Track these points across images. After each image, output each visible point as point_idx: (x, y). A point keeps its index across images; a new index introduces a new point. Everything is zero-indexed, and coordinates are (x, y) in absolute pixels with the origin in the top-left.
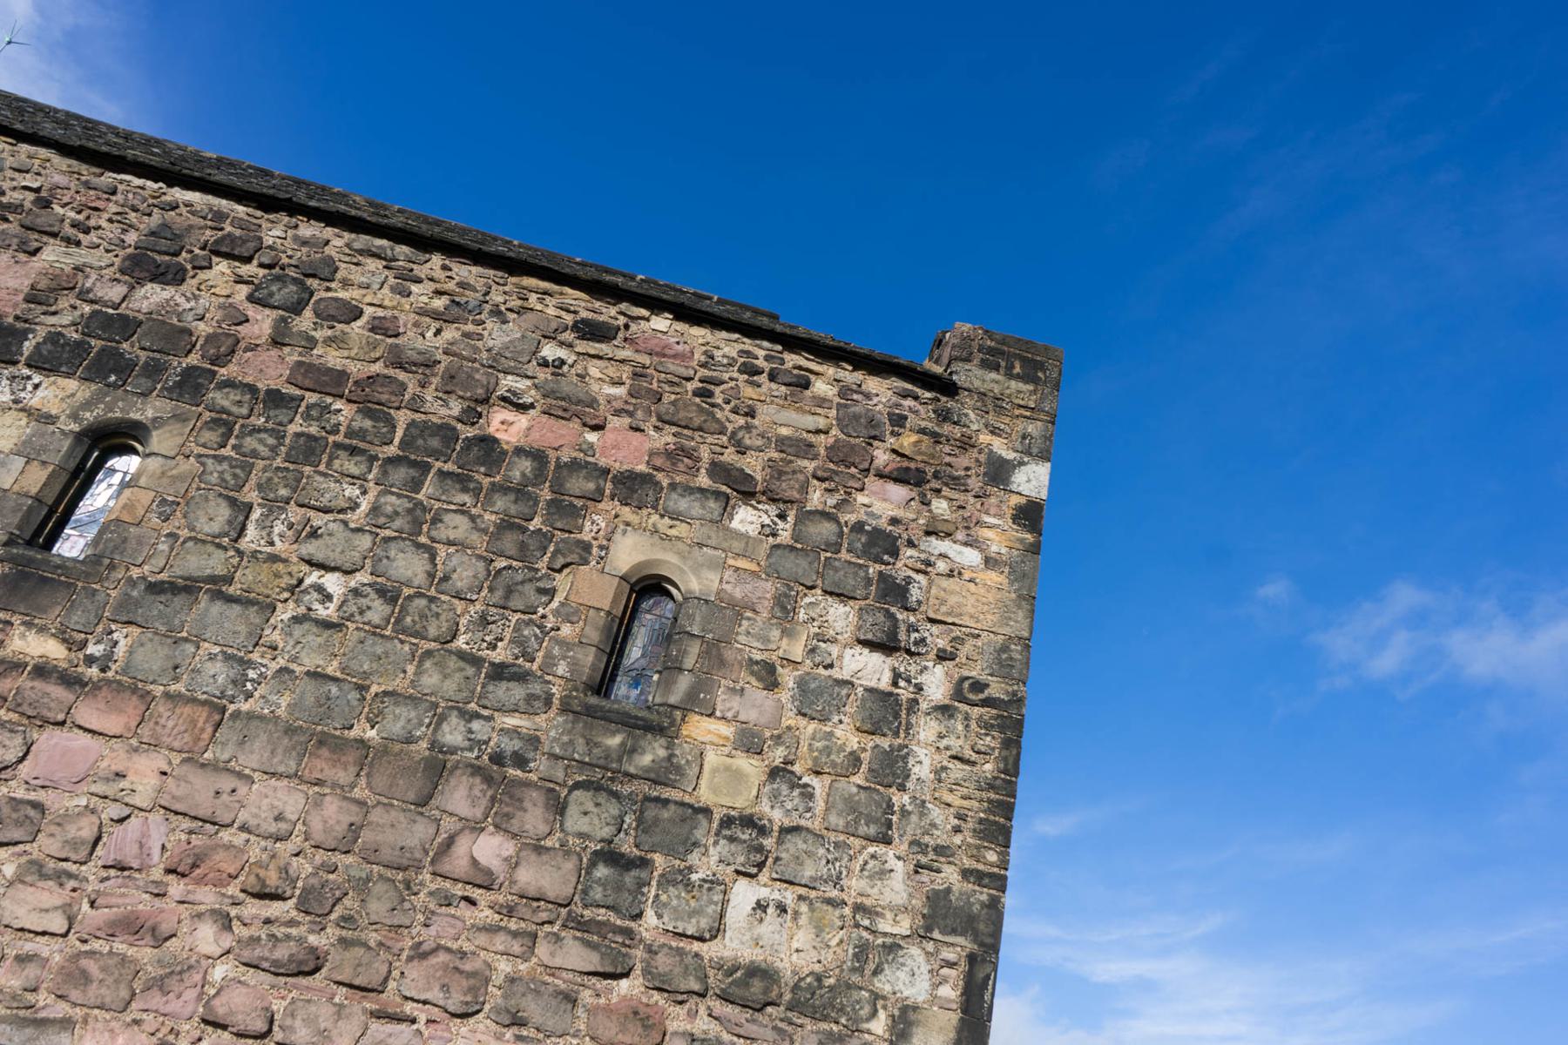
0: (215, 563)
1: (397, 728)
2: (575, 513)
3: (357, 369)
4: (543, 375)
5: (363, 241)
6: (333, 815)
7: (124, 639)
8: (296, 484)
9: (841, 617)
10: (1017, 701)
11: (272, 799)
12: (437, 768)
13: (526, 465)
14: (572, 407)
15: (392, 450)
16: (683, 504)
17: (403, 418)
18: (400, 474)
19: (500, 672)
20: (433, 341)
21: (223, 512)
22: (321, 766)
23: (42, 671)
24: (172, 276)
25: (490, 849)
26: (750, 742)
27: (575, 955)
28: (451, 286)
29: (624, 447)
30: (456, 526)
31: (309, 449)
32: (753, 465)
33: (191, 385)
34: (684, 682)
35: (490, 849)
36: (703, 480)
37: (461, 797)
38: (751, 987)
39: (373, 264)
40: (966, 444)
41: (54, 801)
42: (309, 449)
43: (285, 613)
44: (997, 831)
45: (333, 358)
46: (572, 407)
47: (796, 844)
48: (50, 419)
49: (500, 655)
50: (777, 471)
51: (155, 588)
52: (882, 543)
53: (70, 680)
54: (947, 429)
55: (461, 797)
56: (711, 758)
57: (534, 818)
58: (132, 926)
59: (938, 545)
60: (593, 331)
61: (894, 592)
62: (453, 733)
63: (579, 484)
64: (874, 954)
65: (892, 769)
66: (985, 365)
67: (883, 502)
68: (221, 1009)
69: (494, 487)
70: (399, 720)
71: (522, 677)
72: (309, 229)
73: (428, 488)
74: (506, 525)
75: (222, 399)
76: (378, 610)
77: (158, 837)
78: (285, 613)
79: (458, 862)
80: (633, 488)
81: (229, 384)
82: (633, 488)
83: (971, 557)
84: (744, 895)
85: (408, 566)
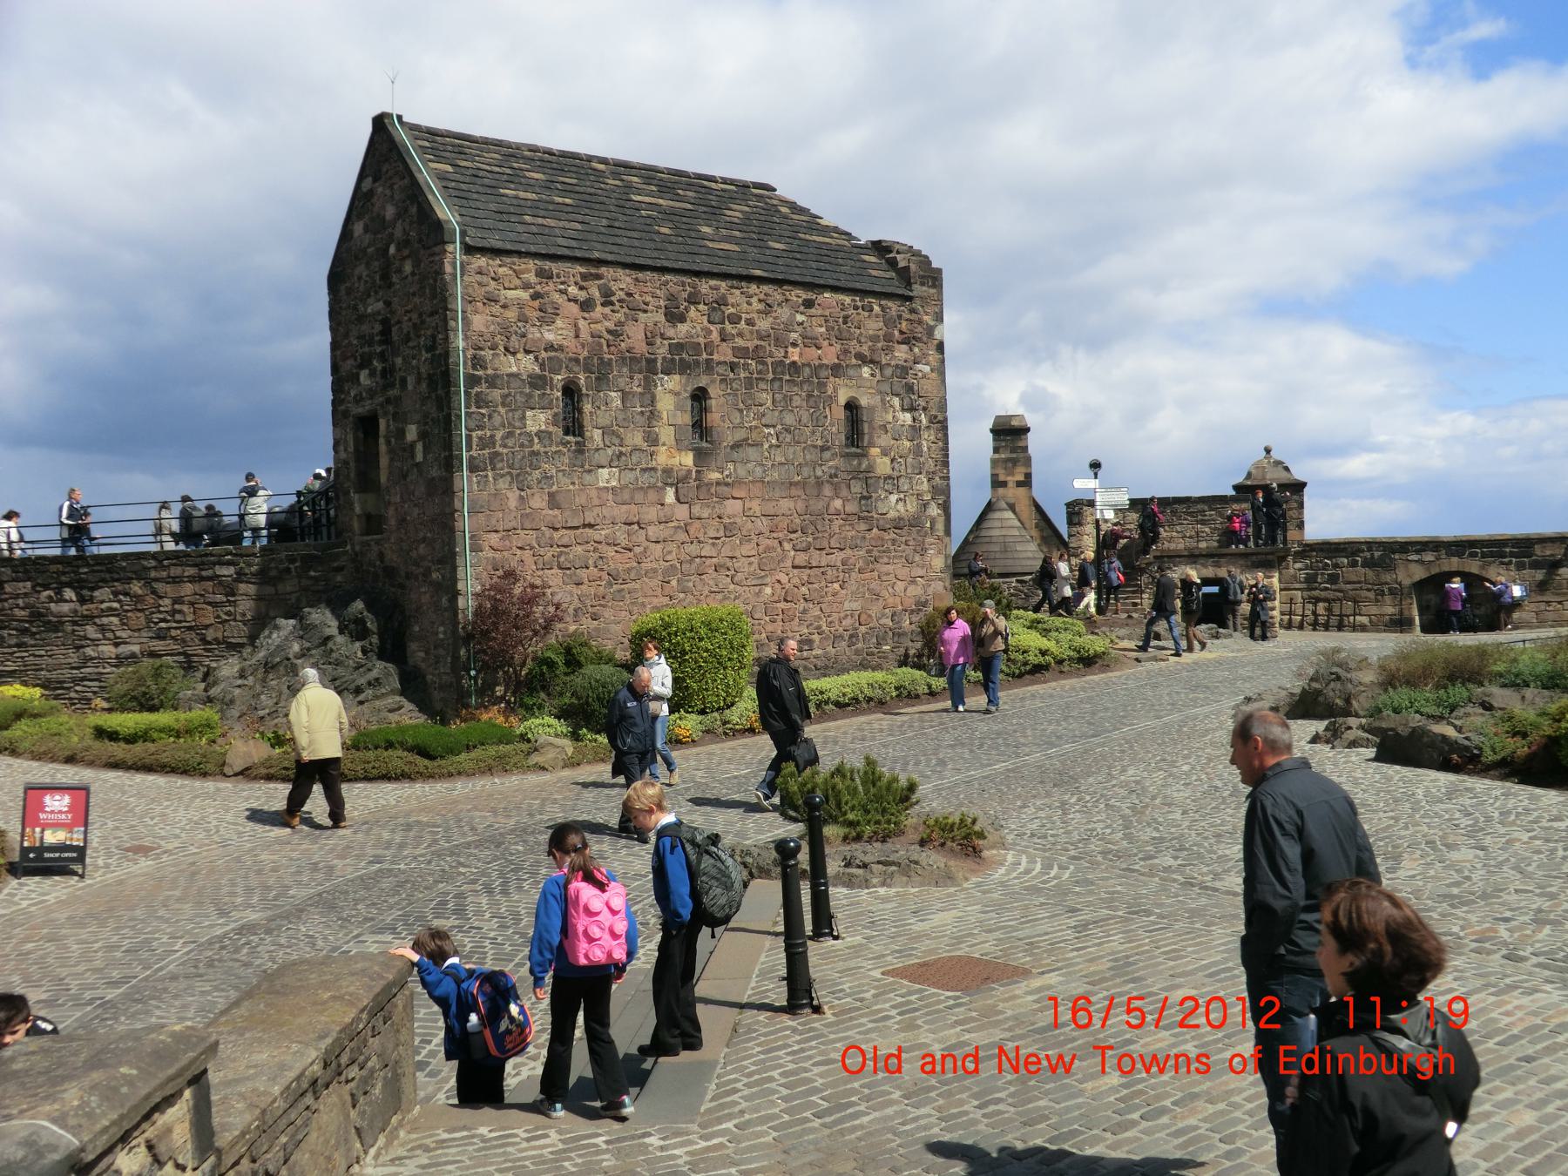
0: (740, 435)
1: (805, 474)
2: (825, 385)
3: (750, 345)
4: (799, 329)
5: (730, 283)
6: (800, 506)
7: (731, 466)
8: (751, 396)
9: (896, 401)
10: (946, 419)
11: (786, 505)
12: (819, 484)
13: (807, 370)
14: (810, 341)
15: (771, 376)
16: (851, 372)
17: (769, 360)
18: (777, 384)
19: (823, 449)
20: (764, 324)
21: (738, 414)
22: (794, 492)
23: (718, 484)
24: (682, 319)
25: (838, 503)
26: (885, 453)
27: (863, 526)
28: (762, 296)
29: (830, 354)
30: (797, 401)
31: (749, 383)
32: (865, 350)
33: (709, 366)
34: (866, 438)
35: (838, 503)
36: (854, 361)
37: (827, 491)
38: (898, 524)
39: (737, 292)
40: (920, 322)
41: (738, 520)
42: (749, 383)
43: (766, 446)
44: (946, 464)
45: (740, 342)
46: (810, 341)
47: (902, 480)
48: (677, 394)
49: (819, 443)
50: (872, 350)
51: (732, 447)
52: (903, 371)
53: (727, 484)
54: (913, 317)
55: (827, 491)
56: (878, 460)
57: (844, 492)
58: (768, 549)
59: (919, 366)
60: (809, 304)
61: (910, 389)
62: (819, 473)
63: (824, 373)
64: (925, 506)
65: (918, 451)
66: (922, 284)
67: (901, 353)
68: (797, 562)
69: (802, 383)
70: (806, 471)
71: (828, 449)
72: (713, 282)
73: (785, 388)
74: (809, 396)
75: (721, 369)
76: (789, 438)
77: (763, 524)
78: (766, 446)
79: (832, 510)
80: (836, 370)
81: (719, 363)
82: (836, 370)
83: (927, 369)
84: (893, 498)
85: (789, 419)
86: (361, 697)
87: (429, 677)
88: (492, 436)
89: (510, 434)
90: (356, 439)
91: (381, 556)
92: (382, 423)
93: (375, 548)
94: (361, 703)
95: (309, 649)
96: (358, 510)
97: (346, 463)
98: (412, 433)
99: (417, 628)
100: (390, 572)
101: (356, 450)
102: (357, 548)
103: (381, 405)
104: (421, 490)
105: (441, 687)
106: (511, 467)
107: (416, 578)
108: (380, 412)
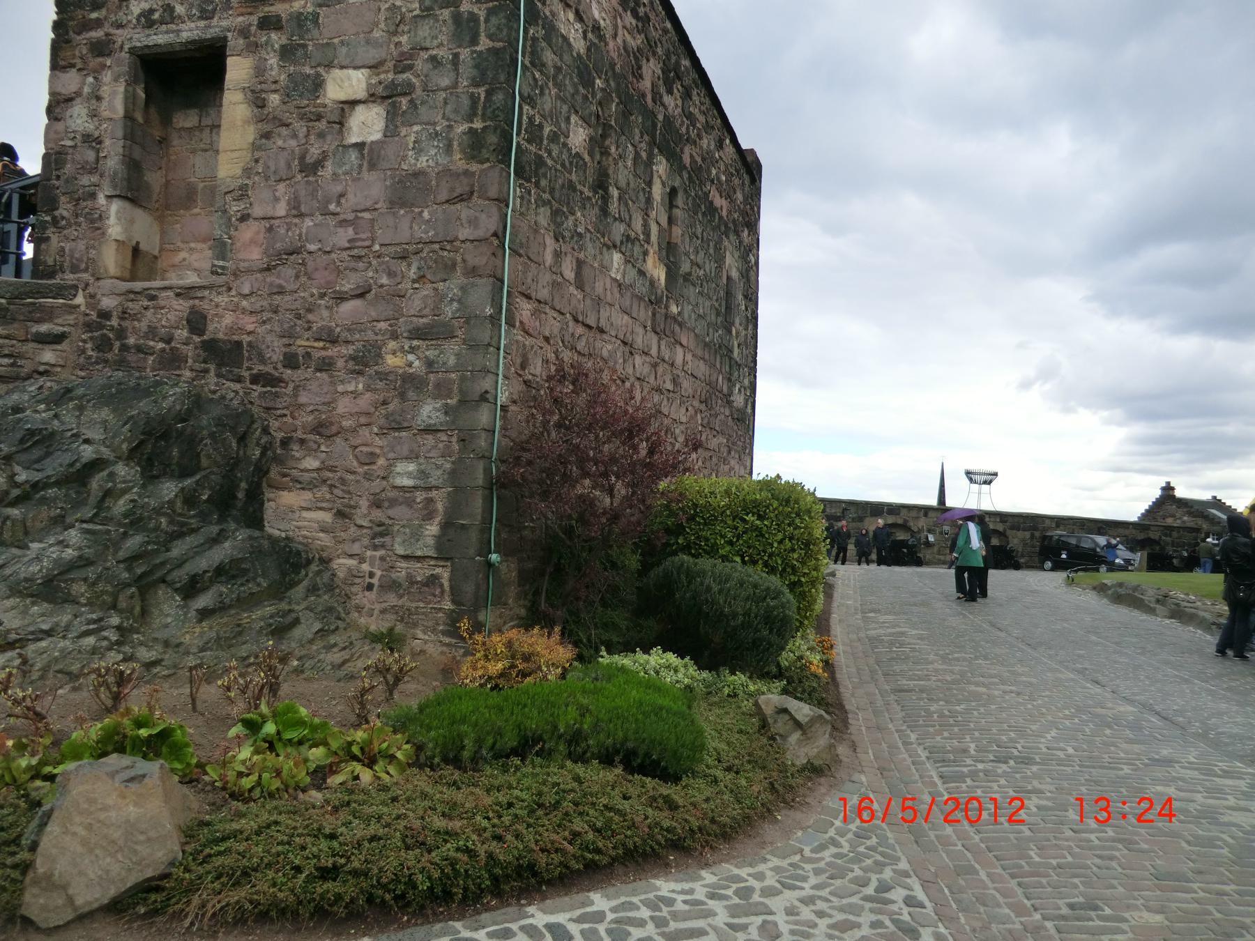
86: (203, 601)
87: (342, 565)
88: (541, 126)
89: (554, 138)
90: (130, 100)
91: (196, 322)
92: (237, 70)
93: (182, 306)
94: (204, 614)
95: (36, 486)
96: (114, 229)
97: (92, 140)
98: (346, 83)
99: (311, 463)
100: (224, 354)
101: (128, 116)
102: (107, 303)
103: (244, 32)
104: (374, 188)
105: (391, 586)
106: (552, 191)
107: (326, 366)
108: (235, 42)
